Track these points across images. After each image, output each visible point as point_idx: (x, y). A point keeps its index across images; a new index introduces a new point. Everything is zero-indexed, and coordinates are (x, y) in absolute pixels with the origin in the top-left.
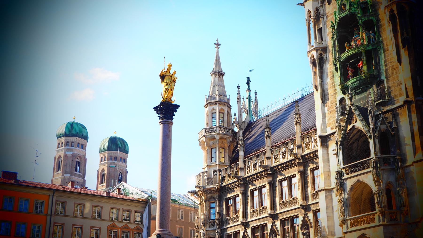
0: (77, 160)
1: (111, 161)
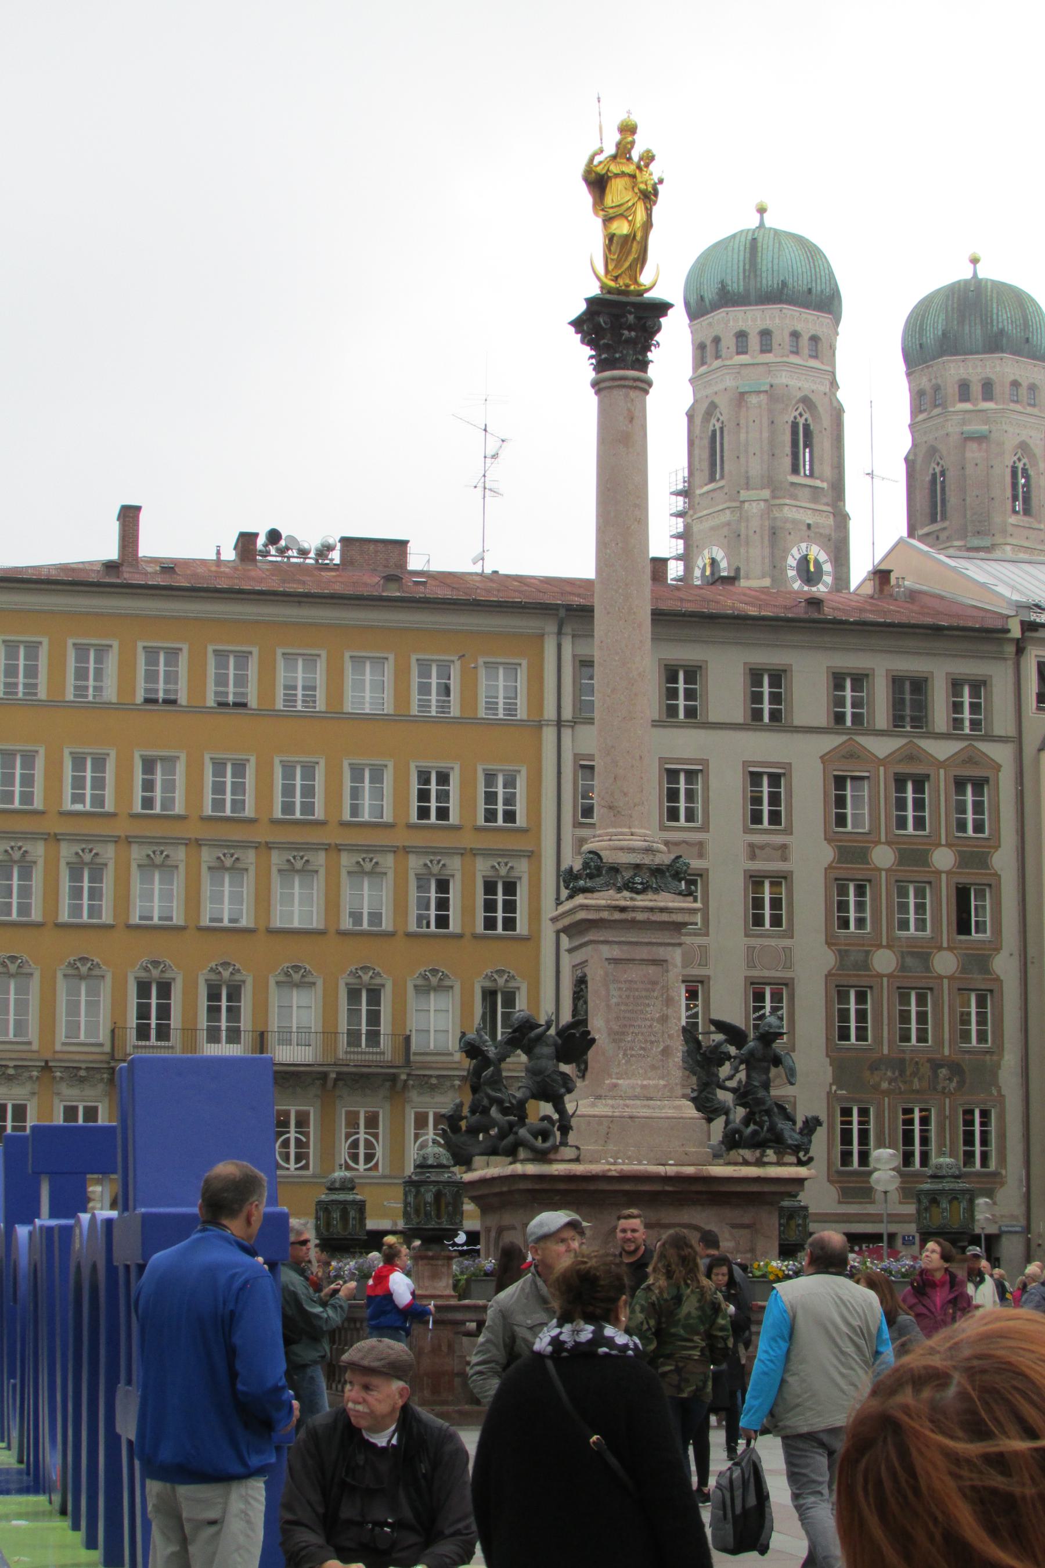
0: (795, 418)
1: (967, 406)
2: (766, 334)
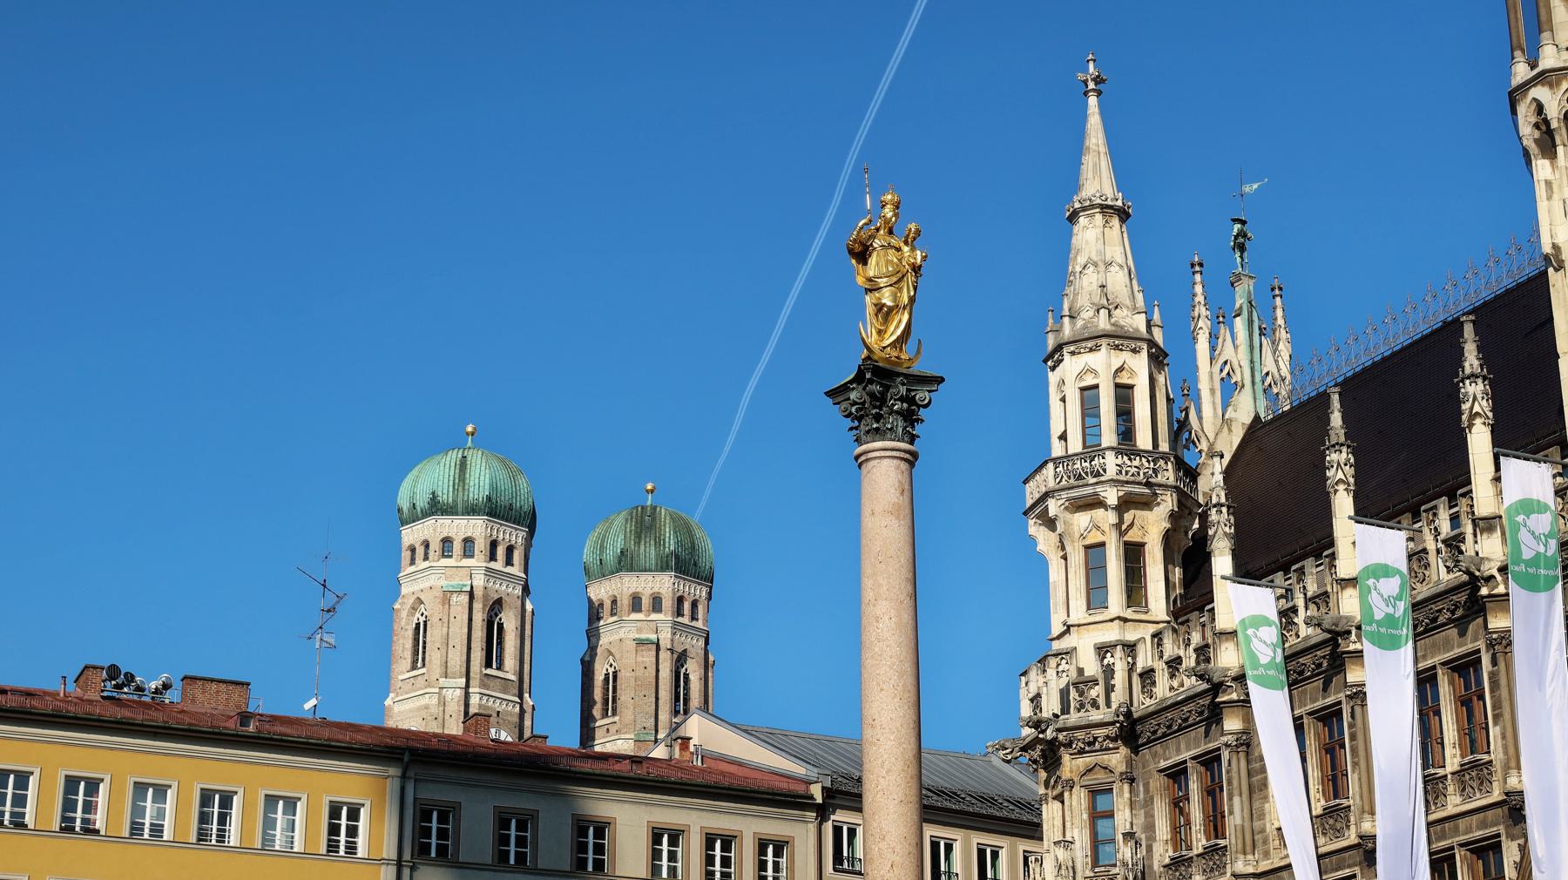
2: (468, 541)
